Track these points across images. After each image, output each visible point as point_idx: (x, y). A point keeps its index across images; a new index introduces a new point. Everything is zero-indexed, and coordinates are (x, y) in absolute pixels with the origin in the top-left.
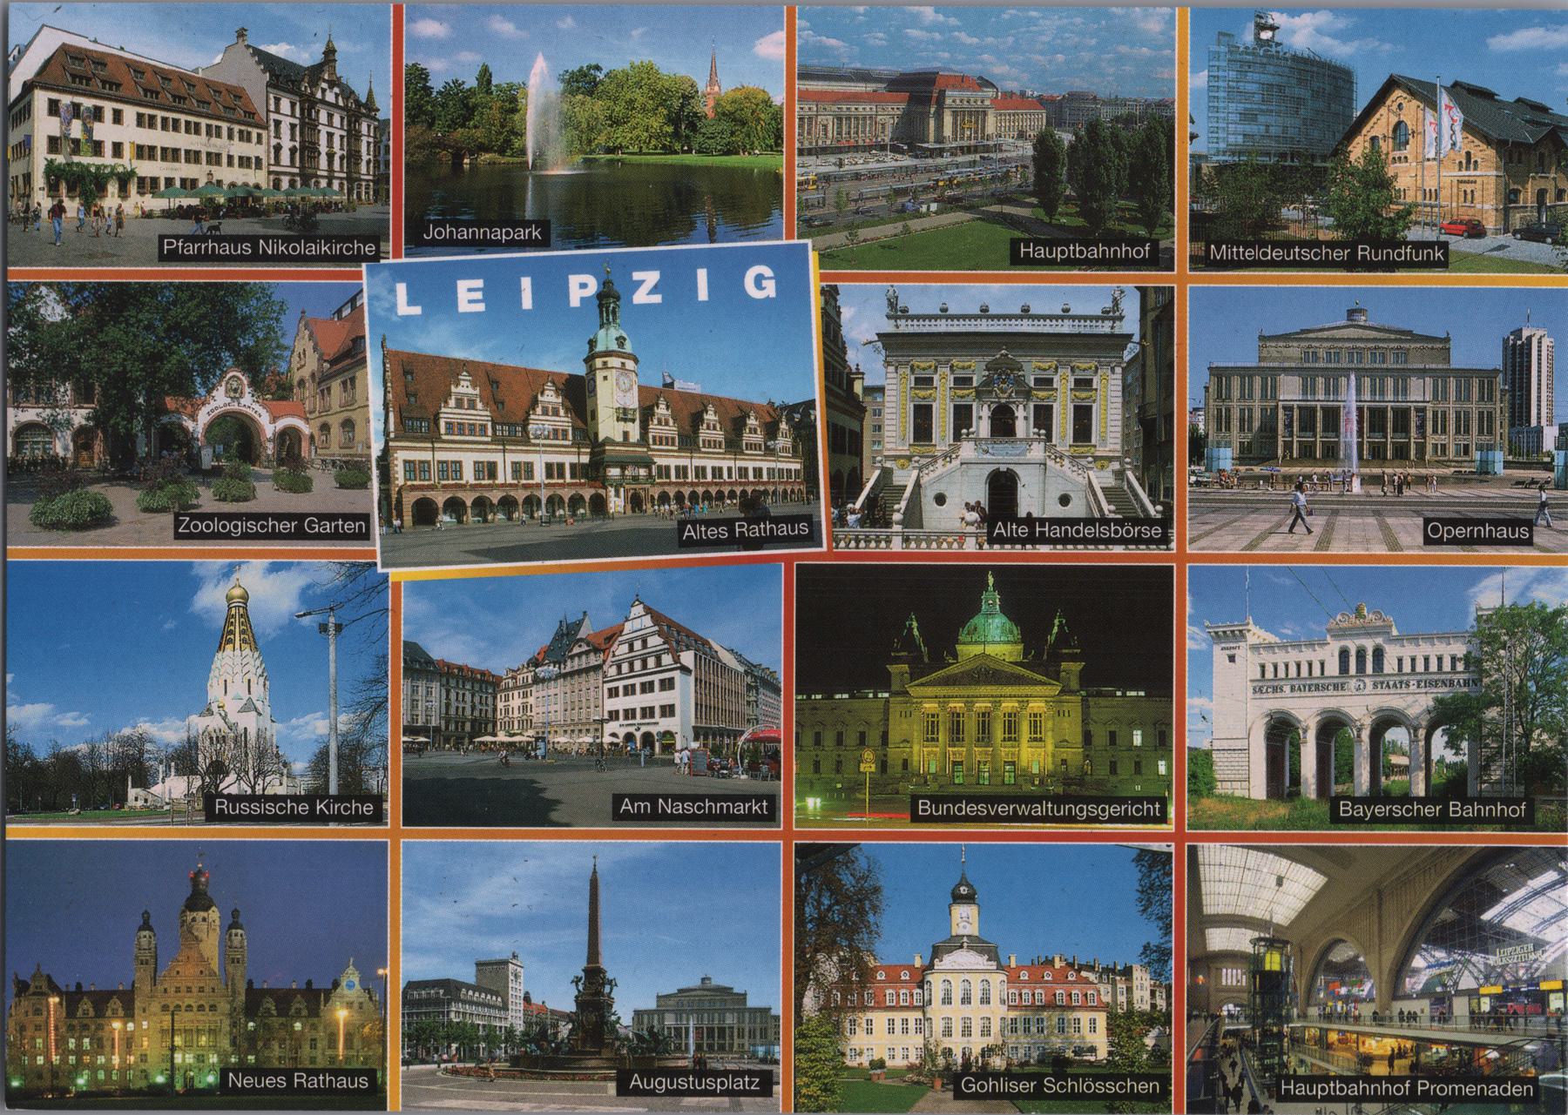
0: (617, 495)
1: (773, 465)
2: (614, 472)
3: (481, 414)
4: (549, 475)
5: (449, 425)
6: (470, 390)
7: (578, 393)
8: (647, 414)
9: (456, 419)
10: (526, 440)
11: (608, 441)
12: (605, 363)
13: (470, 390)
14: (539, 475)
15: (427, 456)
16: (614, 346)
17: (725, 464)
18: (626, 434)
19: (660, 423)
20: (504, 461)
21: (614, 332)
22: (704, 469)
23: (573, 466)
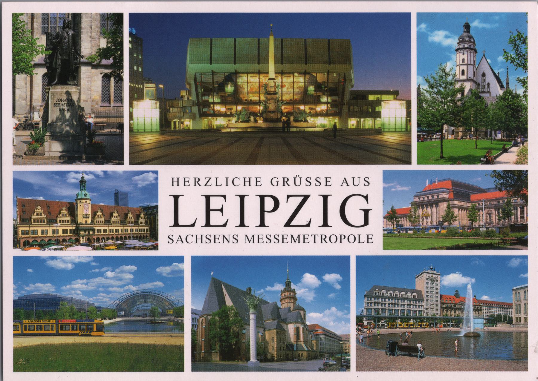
1: (137, 228)
2: (82, 233)
3: (44, 217)
4: (63, 233)
5: (34, 221)
6: (40, 211)
7: (72, 210)
8: (94, 214)
10: (56, 222)
13: (40, 211)
14: (60, 233)
15: (28, 229)
16: (83, 197)
17: (120, 228)
18: (86, 222)
20: (50, 229)
21: (84, 192)
23: (70, 230)
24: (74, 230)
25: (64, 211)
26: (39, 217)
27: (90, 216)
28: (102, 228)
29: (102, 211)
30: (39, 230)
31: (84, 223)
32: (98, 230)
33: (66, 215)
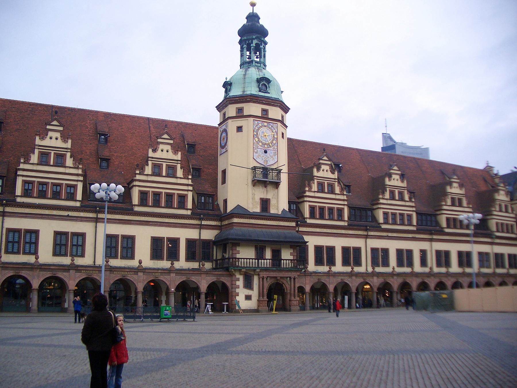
0: (248, 285)
2: (246, 254)
4: (156, 254)
9: (37, 178)
11: (241, 212)
12: (240, 110)
14: (143, 252)
16: (253, 90)
18: (265, 203)
19: (321, 189)
22: (386, 251)
23: (190, 243)
24: (206, 243)
25: (165, 152)
26: (51, 174)
27: (284, 178)
28: (338, 243)
29: (336, 167)
30: (47, 230)
31: (257, 209)
32: (318, 249)
33: (172, 172)
